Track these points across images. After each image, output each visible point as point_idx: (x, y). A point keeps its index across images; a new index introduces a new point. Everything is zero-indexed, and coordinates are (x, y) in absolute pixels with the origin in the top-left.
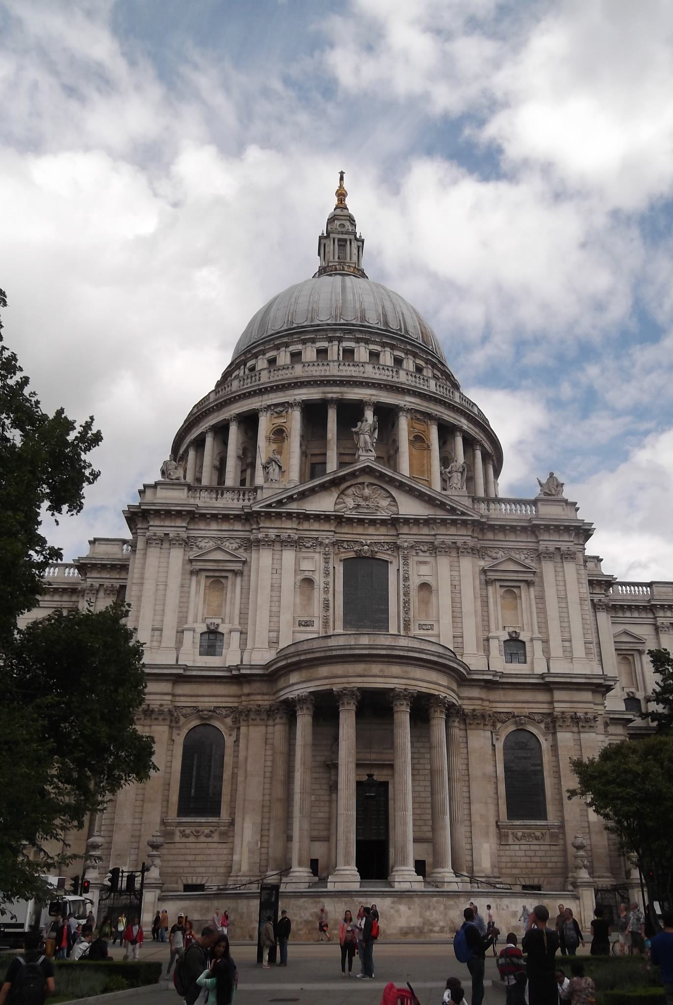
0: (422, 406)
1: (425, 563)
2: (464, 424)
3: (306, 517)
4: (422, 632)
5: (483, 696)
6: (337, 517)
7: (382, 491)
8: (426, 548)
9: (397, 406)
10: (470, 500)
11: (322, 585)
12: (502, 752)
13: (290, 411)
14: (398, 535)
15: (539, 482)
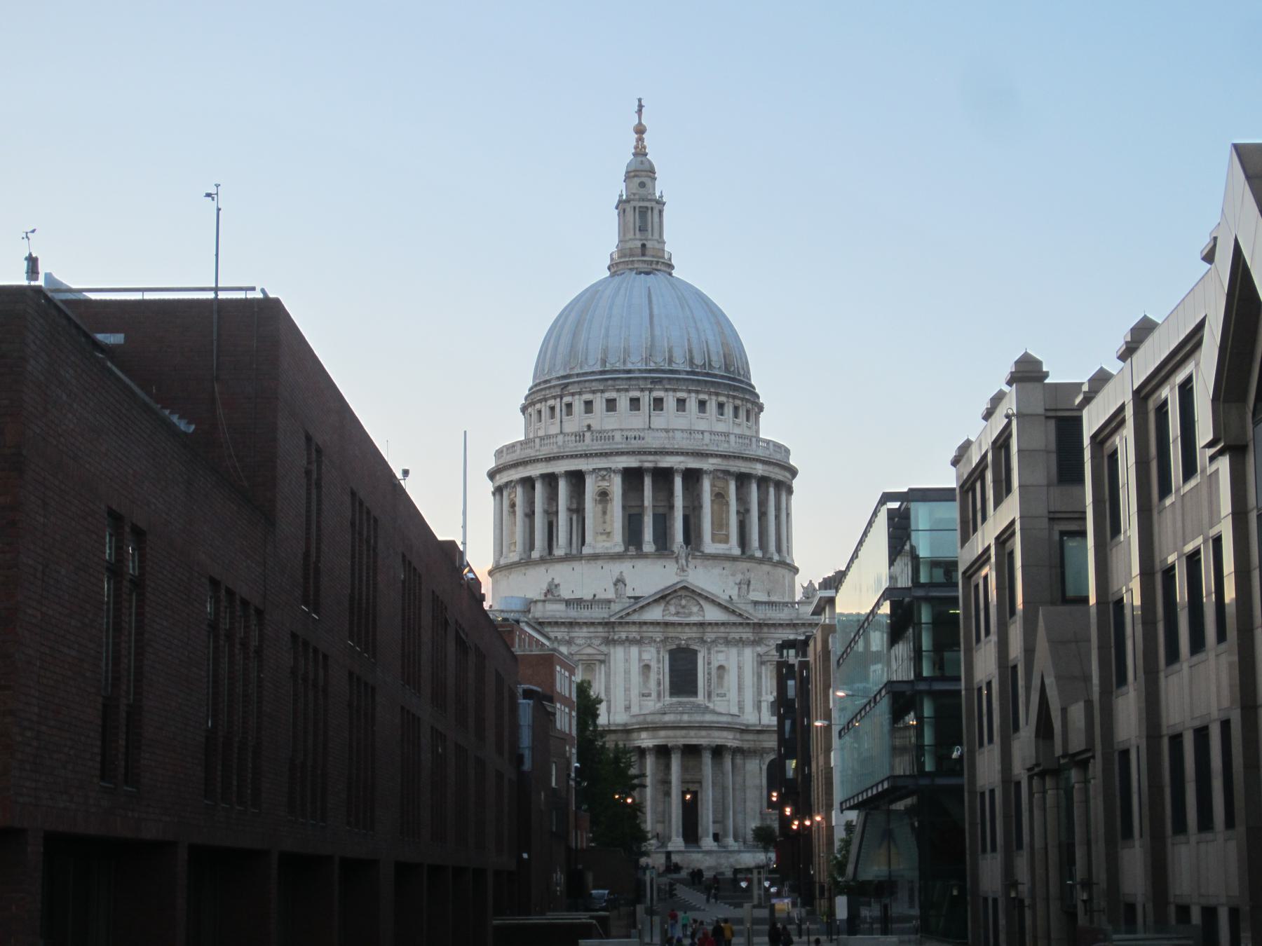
0: (723, 465)
1: (722, 652)
2: (759, 469)
3: (645, 623)
4: (719, 698)
5: (756, 739)
6: (664, 623)
7: (694, 601)
8: (721, 641)
9: (701, 469)
10: (753, 605)
11: (656, 670)
12: (766, 771)
13: (612, 475)
14: (704, 633)
15: (802, 586)
